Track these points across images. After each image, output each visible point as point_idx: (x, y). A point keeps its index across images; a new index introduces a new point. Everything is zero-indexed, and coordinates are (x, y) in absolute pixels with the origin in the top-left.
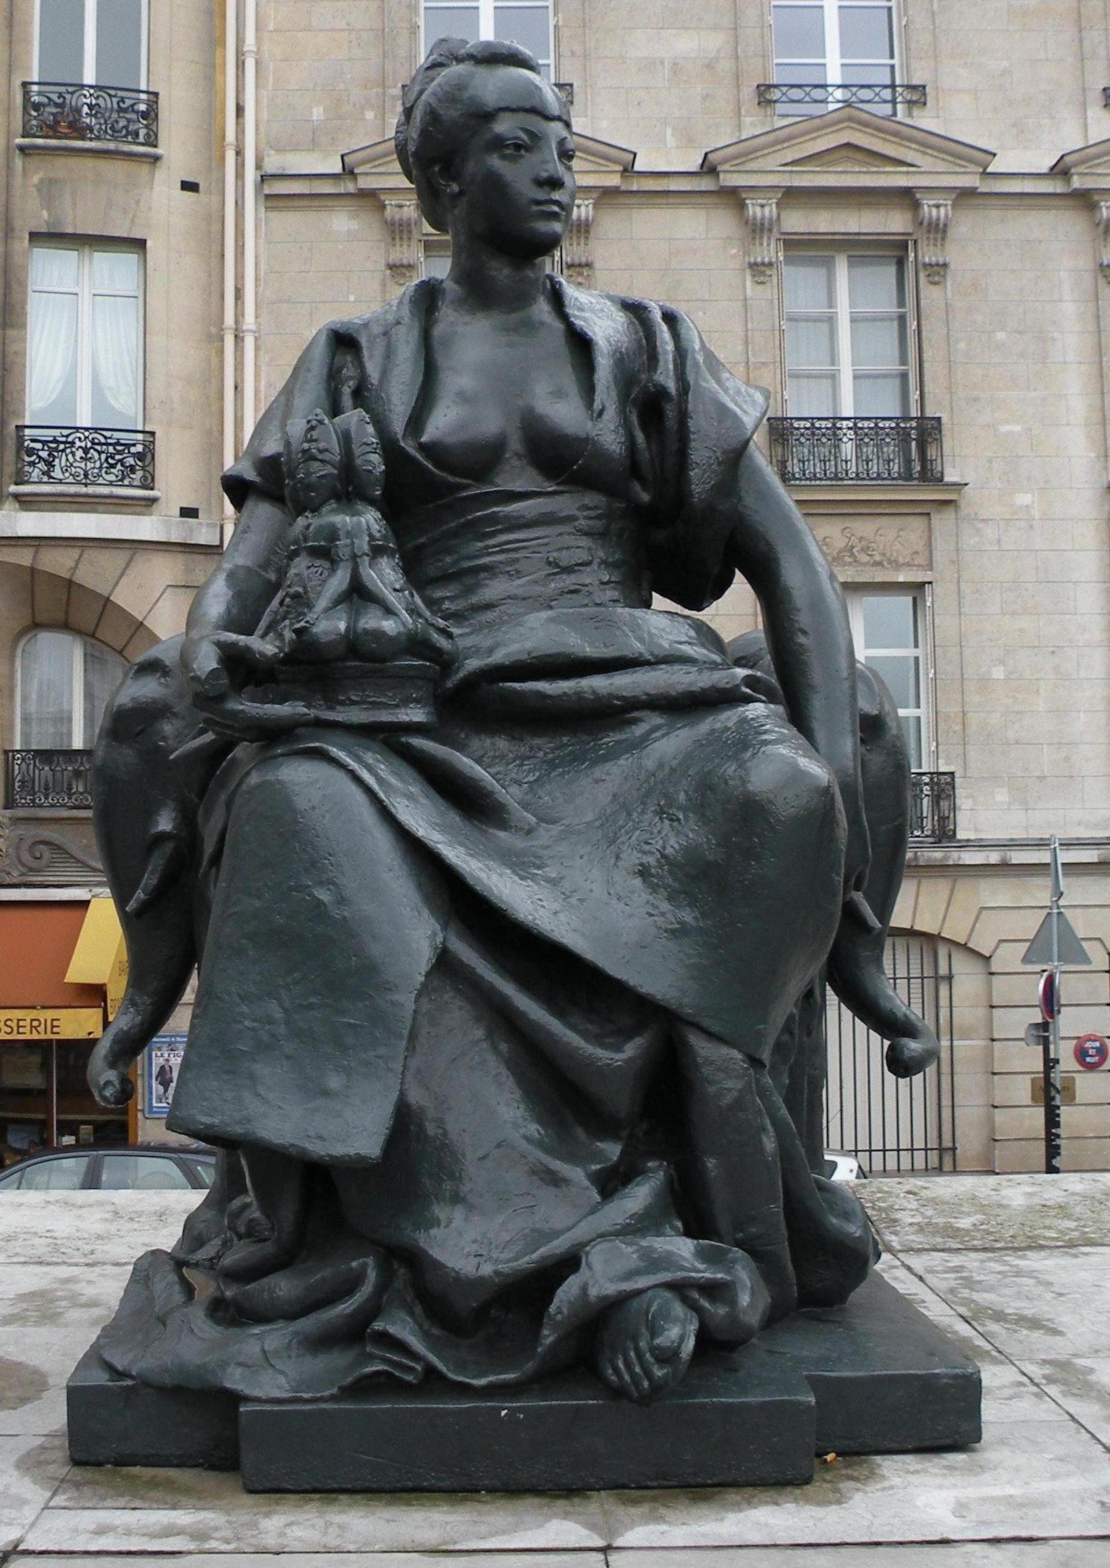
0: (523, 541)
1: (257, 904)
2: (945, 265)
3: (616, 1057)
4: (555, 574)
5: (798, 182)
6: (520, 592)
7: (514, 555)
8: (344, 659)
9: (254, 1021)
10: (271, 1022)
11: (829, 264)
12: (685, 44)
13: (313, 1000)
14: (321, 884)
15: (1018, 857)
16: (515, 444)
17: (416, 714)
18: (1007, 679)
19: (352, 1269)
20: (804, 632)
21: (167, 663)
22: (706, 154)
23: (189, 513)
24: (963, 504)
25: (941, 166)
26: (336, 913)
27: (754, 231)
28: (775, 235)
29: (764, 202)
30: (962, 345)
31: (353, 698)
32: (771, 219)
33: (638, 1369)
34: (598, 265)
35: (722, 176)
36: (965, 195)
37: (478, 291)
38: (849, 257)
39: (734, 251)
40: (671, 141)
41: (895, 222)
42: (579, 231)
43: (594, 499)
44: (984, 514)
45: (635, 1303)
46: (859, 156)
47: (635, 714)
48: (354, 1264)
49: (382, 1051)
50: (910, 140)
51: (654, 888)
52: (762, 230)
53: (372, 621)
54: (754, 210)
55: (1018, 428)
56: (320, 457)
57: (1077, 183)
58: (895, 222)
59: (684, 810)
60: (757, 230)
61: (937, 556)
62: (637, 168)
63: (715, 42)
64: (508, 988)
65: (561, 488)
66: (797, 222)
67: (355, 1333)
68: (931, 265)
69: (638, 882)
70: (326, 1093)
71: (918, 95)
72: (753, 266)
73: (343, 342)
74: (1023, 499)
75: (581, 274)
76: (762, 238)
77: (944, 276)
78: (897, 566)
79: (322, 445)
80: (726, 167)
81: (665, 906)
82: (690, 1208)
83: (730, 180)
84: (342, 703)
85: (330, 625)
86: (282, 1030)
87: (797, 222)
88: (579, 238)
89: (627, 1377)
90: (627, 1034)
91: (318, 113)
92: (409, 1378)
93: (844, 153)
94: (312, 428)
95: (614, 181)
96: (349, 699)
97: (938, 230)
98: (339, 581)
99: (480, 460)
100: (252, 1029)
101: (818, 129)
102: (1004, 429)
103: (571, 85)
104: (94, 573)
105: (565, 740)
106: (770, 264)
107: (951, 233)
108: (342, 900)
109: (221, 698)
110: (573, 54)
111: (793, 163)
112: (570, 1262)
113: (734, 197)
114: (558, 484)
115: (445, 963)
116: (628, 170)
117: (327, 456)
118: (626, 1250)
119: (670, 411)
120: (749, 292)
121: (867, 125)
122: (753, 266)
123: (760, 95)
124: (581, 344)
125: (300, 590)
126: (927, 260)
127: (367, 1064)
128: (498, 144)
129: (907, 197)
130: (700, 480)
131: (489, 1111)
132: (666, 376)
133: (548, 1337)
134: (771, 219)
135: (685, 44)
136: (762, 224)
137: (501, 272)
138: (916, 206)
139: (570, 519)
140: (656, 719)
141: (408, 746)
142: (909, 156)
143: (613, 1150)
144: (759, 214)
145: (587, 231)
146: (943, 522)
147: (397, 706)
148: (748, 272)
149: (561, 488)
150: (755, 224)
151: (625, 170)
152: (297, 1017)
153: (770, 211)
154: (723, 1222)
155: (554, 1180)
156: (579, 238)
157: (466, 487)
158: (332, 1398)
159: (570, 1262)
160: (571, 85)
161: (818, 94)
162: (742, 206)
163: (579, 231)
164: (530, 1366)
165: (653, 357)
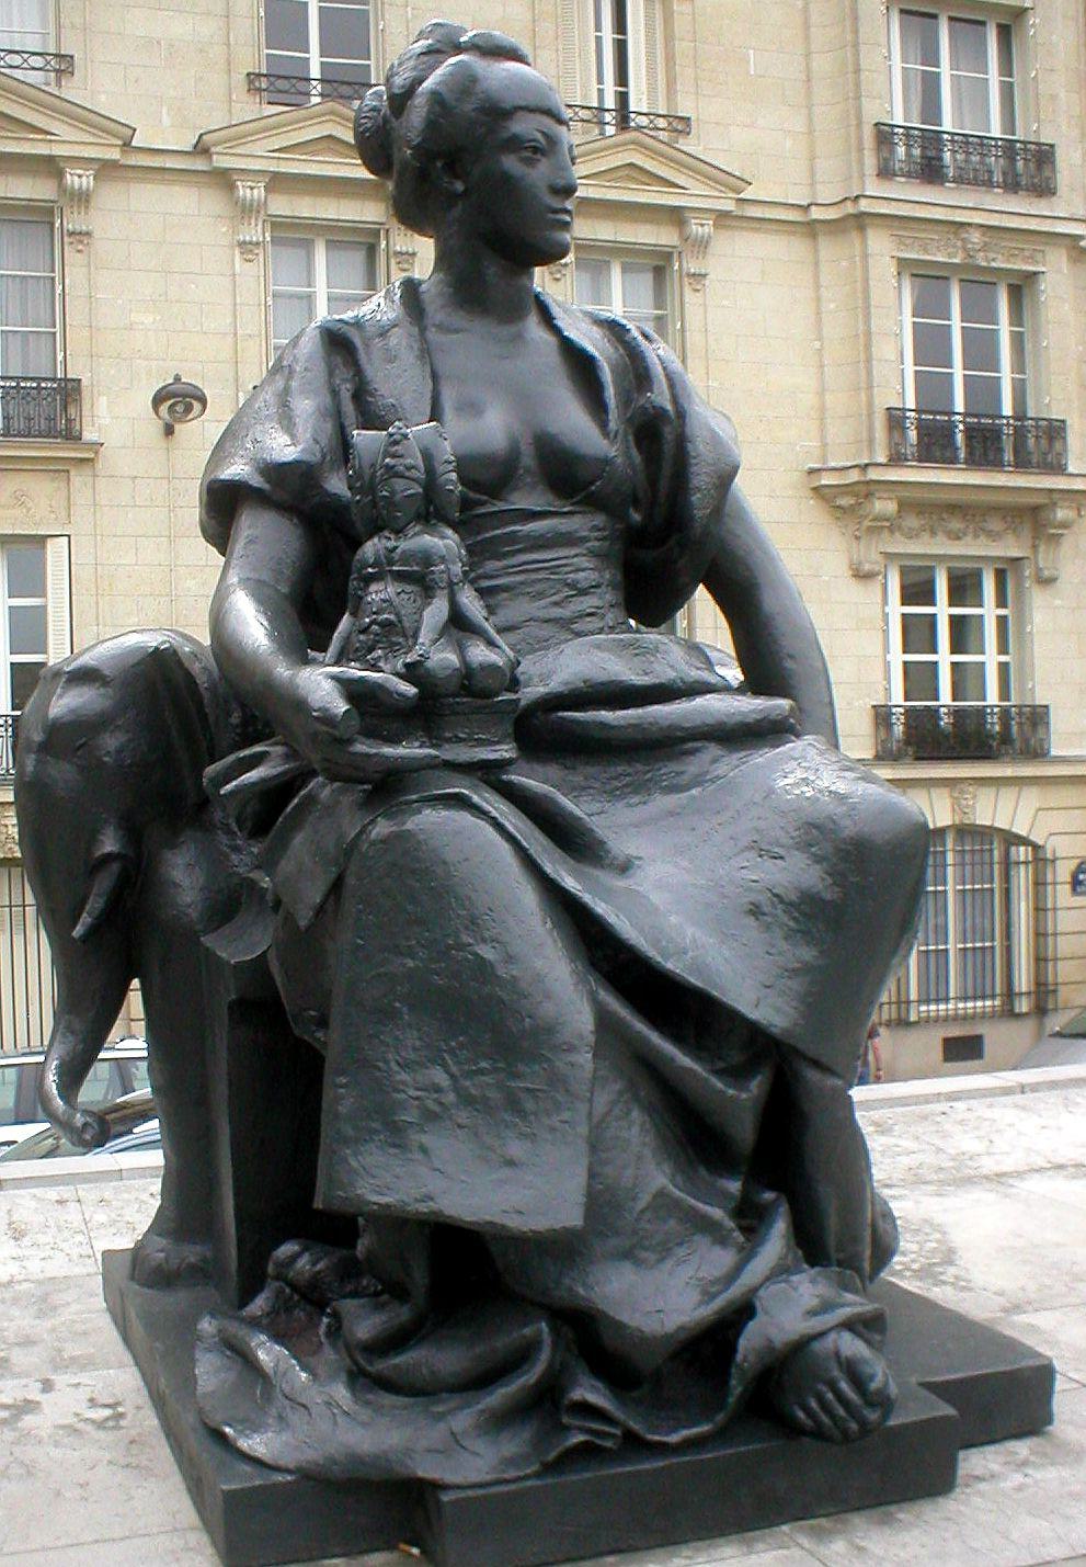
0: (543, 561)
1: (411, 963)
2: (414, 254)
4: (572, 596)
6: (542, 614)
7: (534, 576)
8: (454, 695)
9: (418, 1089)
10: (438, 1089)
11: (307, 245)
13: (484, 1064)
14: (484, 940)
16: (528, 459)
17: (506, 751)
19: (524, 1337)
20: (791, 657)
21: (107, 672)
22: (201, 135)
26: (501, 972)
27: (243, 211)
28: (262, 216)
29: (253, 185)
31: (461, 735)
32: (259, 200)
33: (841, 1412)
34: (97, 234)
35: (215, 157)
38: (327, 241)
39: (224, 229)
40: (166, 121)
42: (80, 200)
43: (600, 519)
45: (816, 1346)
47: (690, 745)
48: (527, 1331)
49: (566, 1115)
51: (768, 927)
52: (251, 211)
53: (479, 653)
54: (243, 191)
56: (407, 474)
59: (788, 848)
62: (133, 144)
63: (209, 28)
65: (578, 509)
66: (281, 206)
68: (401, 253)
69: (751, 921)
70: (511, 1163)
73: (339, 343)
75: (81, 242)
76: (250, 218)
77: (412, 264)
79: (409, 461)
80: (219, 149)
81: (783, 945)
84: (449, 740)
85: (443, 658)
86: (451, 1098)
87: (281, 206)
88: (79, 207)
89: (825, 1419)
92: (609, 1444)
93: (324, 144)
94: (396, 443)
95: (114, 154)
96: (456, 737)
100: (417, 1098)
101: (306, 119)
103: (72, 57)
105: (620, 769)
106: (258, 244)
108: (510, 959)
109: (350, 741)
110: (73, 26)
111: (279, 150)
113: (224, 180)
114: (572, 504)
116: (126, 144)
117: (414, 473)
119: (668, 433)
120: (237, 266)
122: (242, 244)
123: (251, 82)
124: (579, 363)
125: (392, 617)
126: (398, 248)
127: (553, 1129)
134: (259, 200)
135: (180, 28)
136: (251, 205)
139: (584, 540)
140: (714, 750)
141: (510, 784)
144: (248, 195)
145: (87, 201)
147: (498, 743)
148: (237, 251)
149: (578, 509)
150: (244, 205)
151: (124, 145)
152: (468, 1083)
153: (259, 193)
156: (79, 207)
157: (483, 504)
158: (537, 1475)
160: (72, 57)
161: (301, 86)
162: (232, 187)
163: (80, 200)
164: (720, 1417)
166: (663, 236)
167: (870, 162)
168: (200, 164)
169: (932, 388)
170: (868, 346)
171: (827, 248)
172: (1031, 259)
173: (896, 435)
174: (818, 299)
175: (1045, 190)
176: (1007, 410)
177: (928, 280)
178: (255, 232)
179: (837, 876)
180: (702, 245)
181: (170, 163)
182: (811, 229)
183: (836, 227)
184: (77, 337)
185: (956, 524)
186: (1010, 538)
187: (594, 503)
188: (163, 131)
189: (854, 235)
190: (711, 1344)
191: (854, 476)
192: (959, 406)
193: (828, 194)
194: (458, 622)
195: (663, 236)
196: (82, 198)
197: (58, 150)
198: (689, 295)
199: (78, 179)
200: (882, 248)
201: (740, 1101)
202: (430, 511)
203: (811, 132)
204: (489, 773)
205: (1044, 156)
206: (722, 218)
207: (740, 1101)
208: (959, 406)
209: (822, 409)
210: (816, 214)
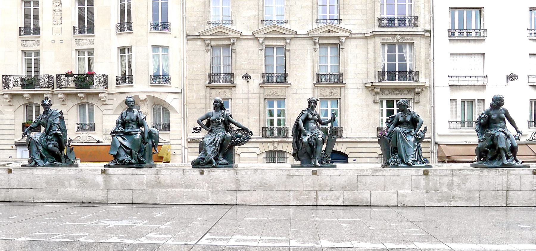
3: (128, 151)
5: (267, 36)
12: (250, 14)
15: (358, 140)
23: (176, 88)
54: (260, 41)
63: (255, 13)
71: (286, 22)
78: (281, 96)
83: (256, 36)
91: (195, 25)
95: (239, 36)
97: (288, 44)
104: (162, 97)
113: (257, 39)
129: (283, 38)
135: (250, 14)
166: (336, 42)
167: (376, 24)
168: (253, 37)
169: (391, 66)
172: (412, 39)
173: (381, 77)
181: (248, 37)
182: (366, 38)
184: (233, 67)
185: (397, 92)
186: (409, 95)
188: (247, 32)
191: (371, 84)
192: (397, 70)
193: (369, 31)
195: (336, 42)
196: (234, 44)
197: (230, 37)
199: (233, 41)
200: (378, 40)
205: (416, 19)
206: (347, 38)
208: (397, 70)
210: (366, 35)
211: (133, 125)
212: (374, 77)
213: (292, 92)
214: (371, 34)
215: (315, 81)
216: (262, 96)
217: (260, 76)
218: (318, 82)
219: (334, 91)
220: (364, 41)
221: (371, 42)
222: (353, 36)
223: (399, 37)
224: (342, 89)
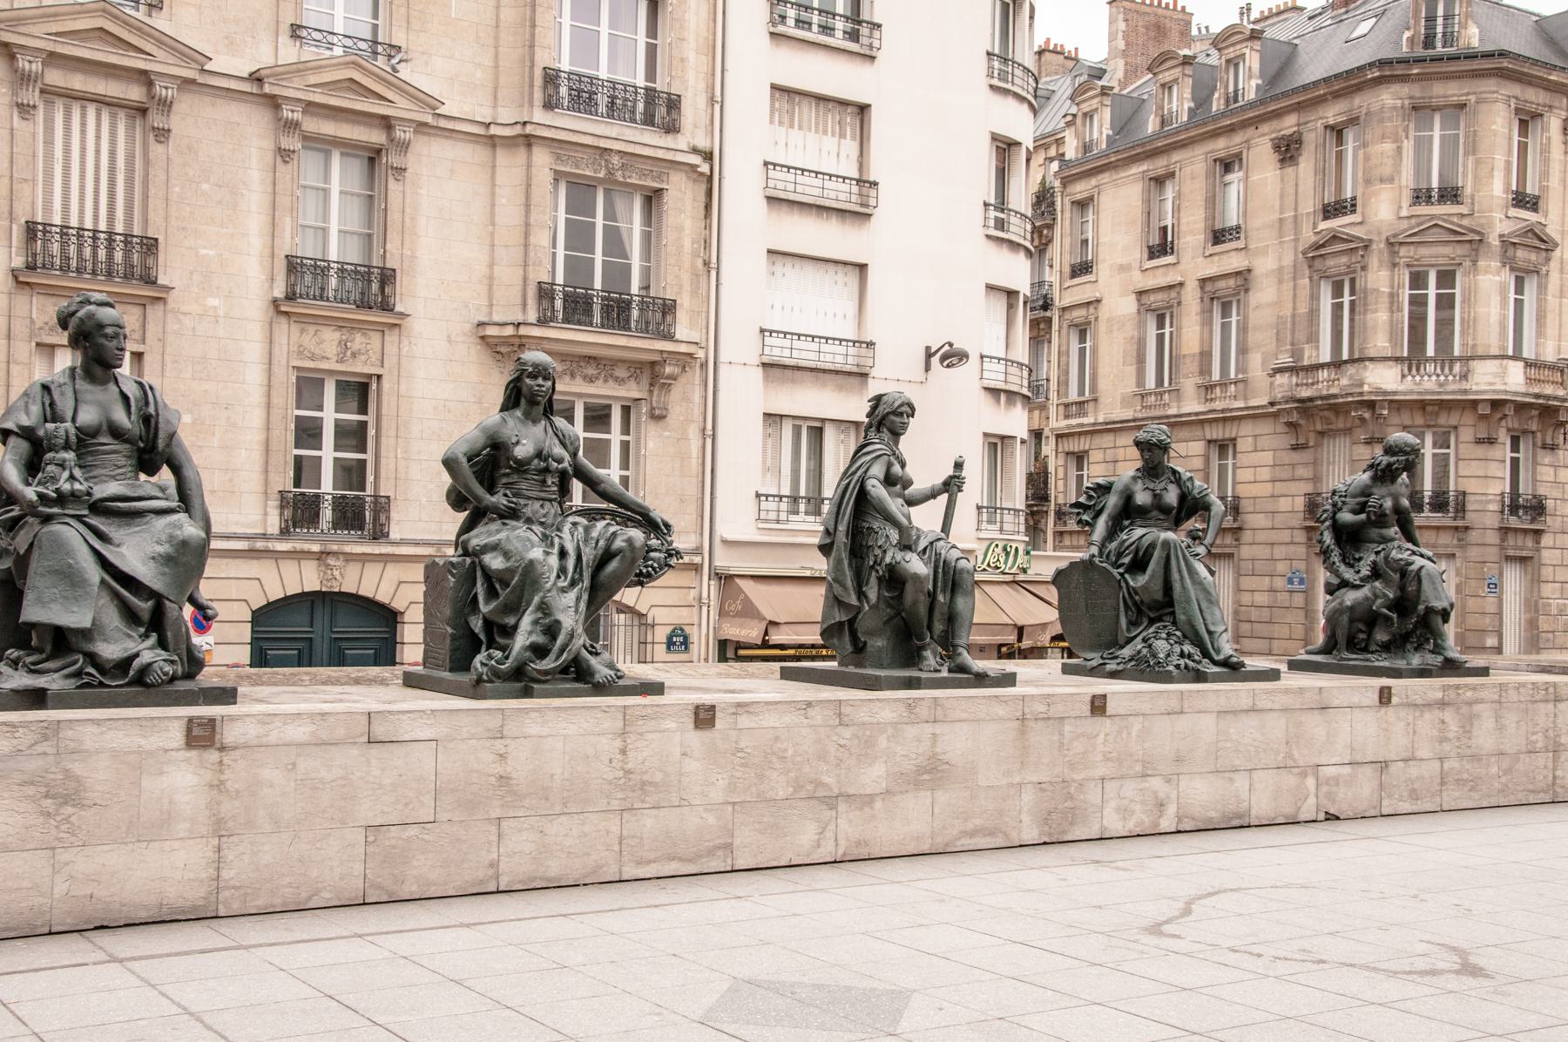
5: (60, 49)
16: (105, 428)
17: (85, 512)
18: (194, 423)
24: (170, 300)
25: (171, 60)
28: (39, 84)
30: (177, 189)
36: (187, 83)
37: (89, 376)
41: (135, 93)
44: (184, 309)
46: (110, 39)
50: (150, 35)
53: (77, 486)
54: (23, 63)
55: (212, 253)
57: (267, 89)
58: (135, 93)
60: (25, 79)
61: (149, 334)
64: (118, 587)
66: (55, 77)
67: (78, 674)
72: (20, 106)
74: (213, 302)
82: (162, 644)
85: (66, 487)
90: (147, 600)
93: (97, 34)
97: (166, 105)
98: (66, 474)
99: (93, 432)
102: (203, 252)
107: (175, 107)
111: (56, 34)
112: (137, 655)
115: (103, 581)
118: (149, 653)
121: (117, 18)
122: (20, 106)
124: (125, 398)
128: (106, 336)
129: (146, 78)
130: (161, 444)
131: (112, 618)
132: (151, 410)
133: (132, 673)
137: (98, 371)
138: (150, 84)
142: (148, 47)
143: (142, 630)
146: (154, 312)
154: (171, 646)
155: (130, 636)
159: (137, 655)
165: (147, 403)
166: (376, 137)
167: (538, 96)
169: (578, 268)
170: (527, 235)
171: (502, 157)
172: (659, 178)
173: (545, 303)
174: (493, 194)
175: (672, 128)
176: (635, 289)
177: (580, 192)
178: (32, 96)
179: (177, 551)
180: (404, 146)
182: (492, 142)
183: (510, 142)
185: (591, 371)
186: (633, 384)
187: (126, 441)
189: (522, 151)
190: (124, 664)
191: (509, 331)
192: (598, 285)
193: (506, 115)
194: (72, 477)
195: (376, 137)
198: (392, 184)
201: (144, 606)
202: (67, 446)
203: (496, 67)
204: (79, 518)
205: (674, 103)
207: (144, 606)
208: (598, 285)
209: (491, 278)
210: (494, 130)
211: (118, 456)
212: (519, 300)
213: (172, 326)
214: (518, 130)
215: (279, 291)
216: (20, 328)
217: (17, 233)
218: (291, 297)
219: (358, 341)
220: (479, 153)
221: (510, 166)
222: (443, 123)
223: (616, 160)
224: (391, 338)
